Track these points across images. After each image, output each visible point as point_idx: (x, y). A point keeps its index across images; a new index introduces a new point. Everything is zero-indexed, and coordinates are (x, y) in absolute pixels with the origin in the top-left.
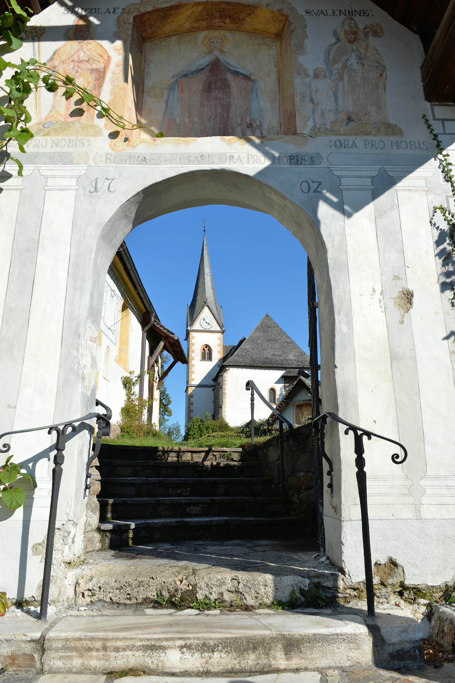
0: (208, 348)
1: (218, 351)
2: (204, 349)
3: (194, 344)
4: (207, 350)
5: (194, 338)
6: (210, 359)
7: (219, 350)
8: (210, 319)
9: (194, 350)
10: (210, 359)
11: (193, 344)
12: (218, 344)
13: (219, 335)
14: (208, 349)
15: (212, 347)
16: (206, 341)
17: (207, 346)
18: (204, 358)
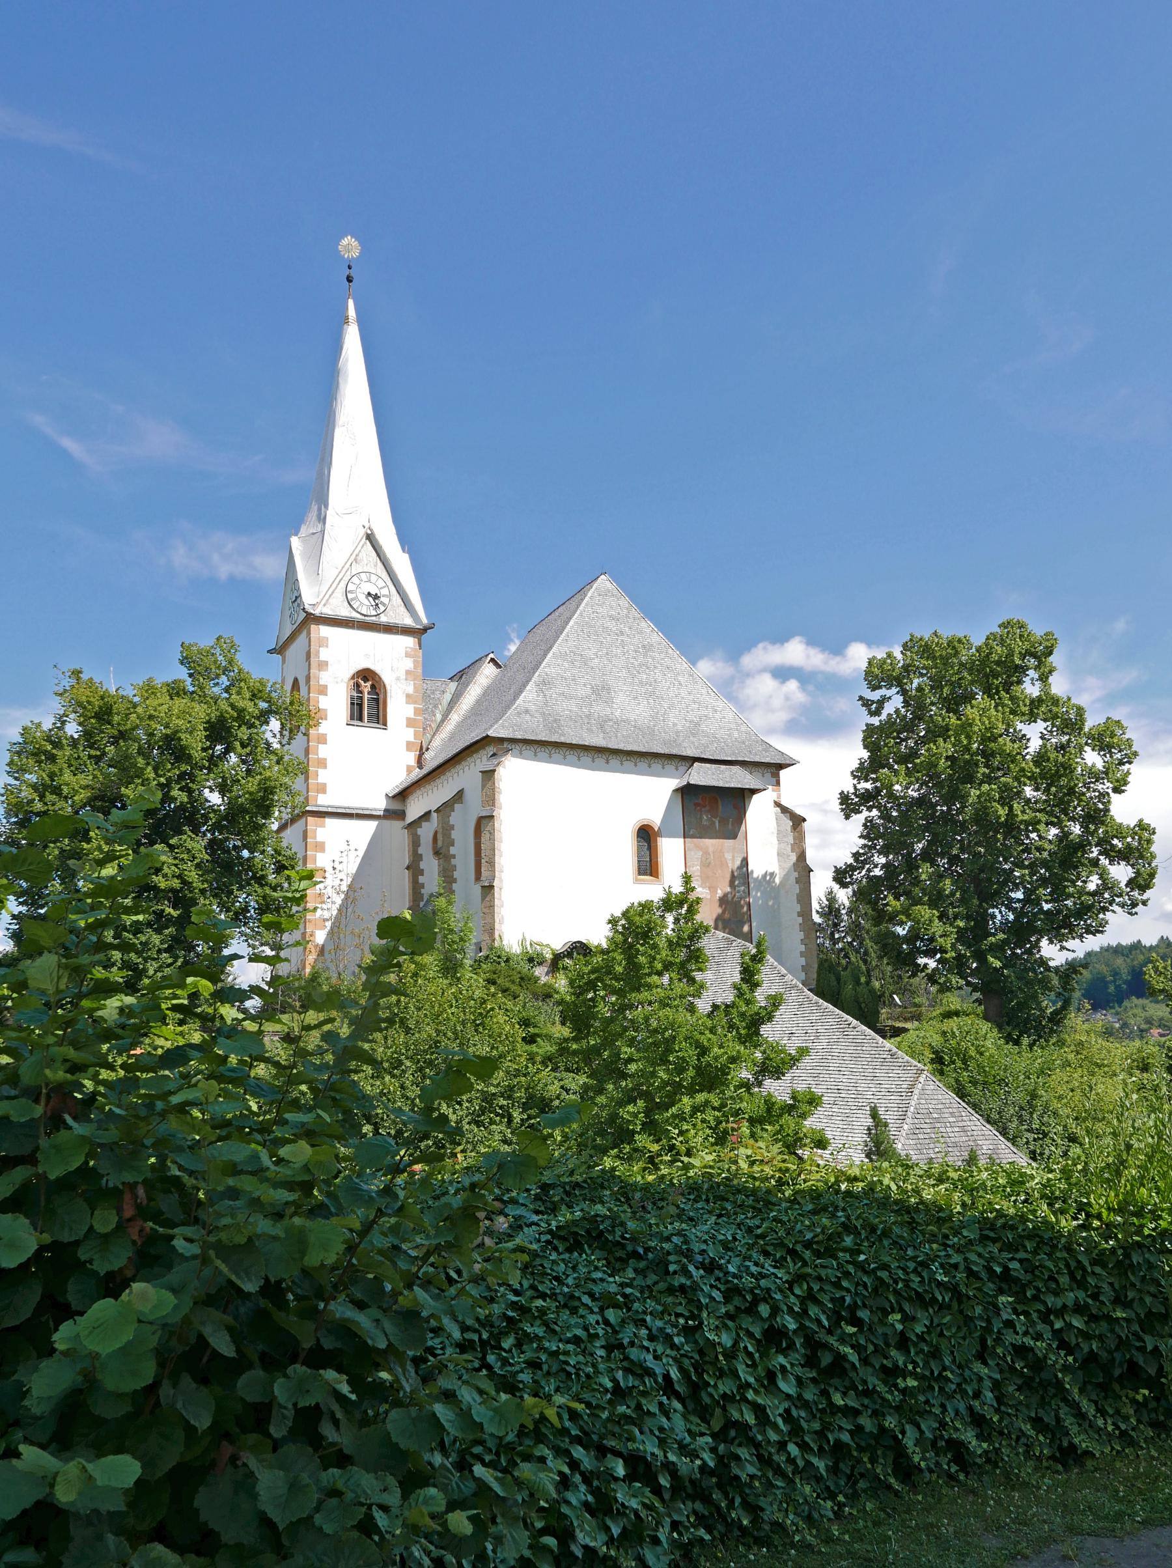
0: (369, 684)
1: (408, 696)
2: (358, 685)
3: (326, 663)
4: (366, 687)
5: (324, 642)
6: (379, 718)
7: (410, 689)
8: (381, 583)
9: (326, 687)
10: (379, 718)
11: (323, 665)
12: (408, 672)
13: (409, 641)
14: (373, 687)
15: (387, 677)
16: (367, 656)
17: (366, 675)
18: (356, 713)
